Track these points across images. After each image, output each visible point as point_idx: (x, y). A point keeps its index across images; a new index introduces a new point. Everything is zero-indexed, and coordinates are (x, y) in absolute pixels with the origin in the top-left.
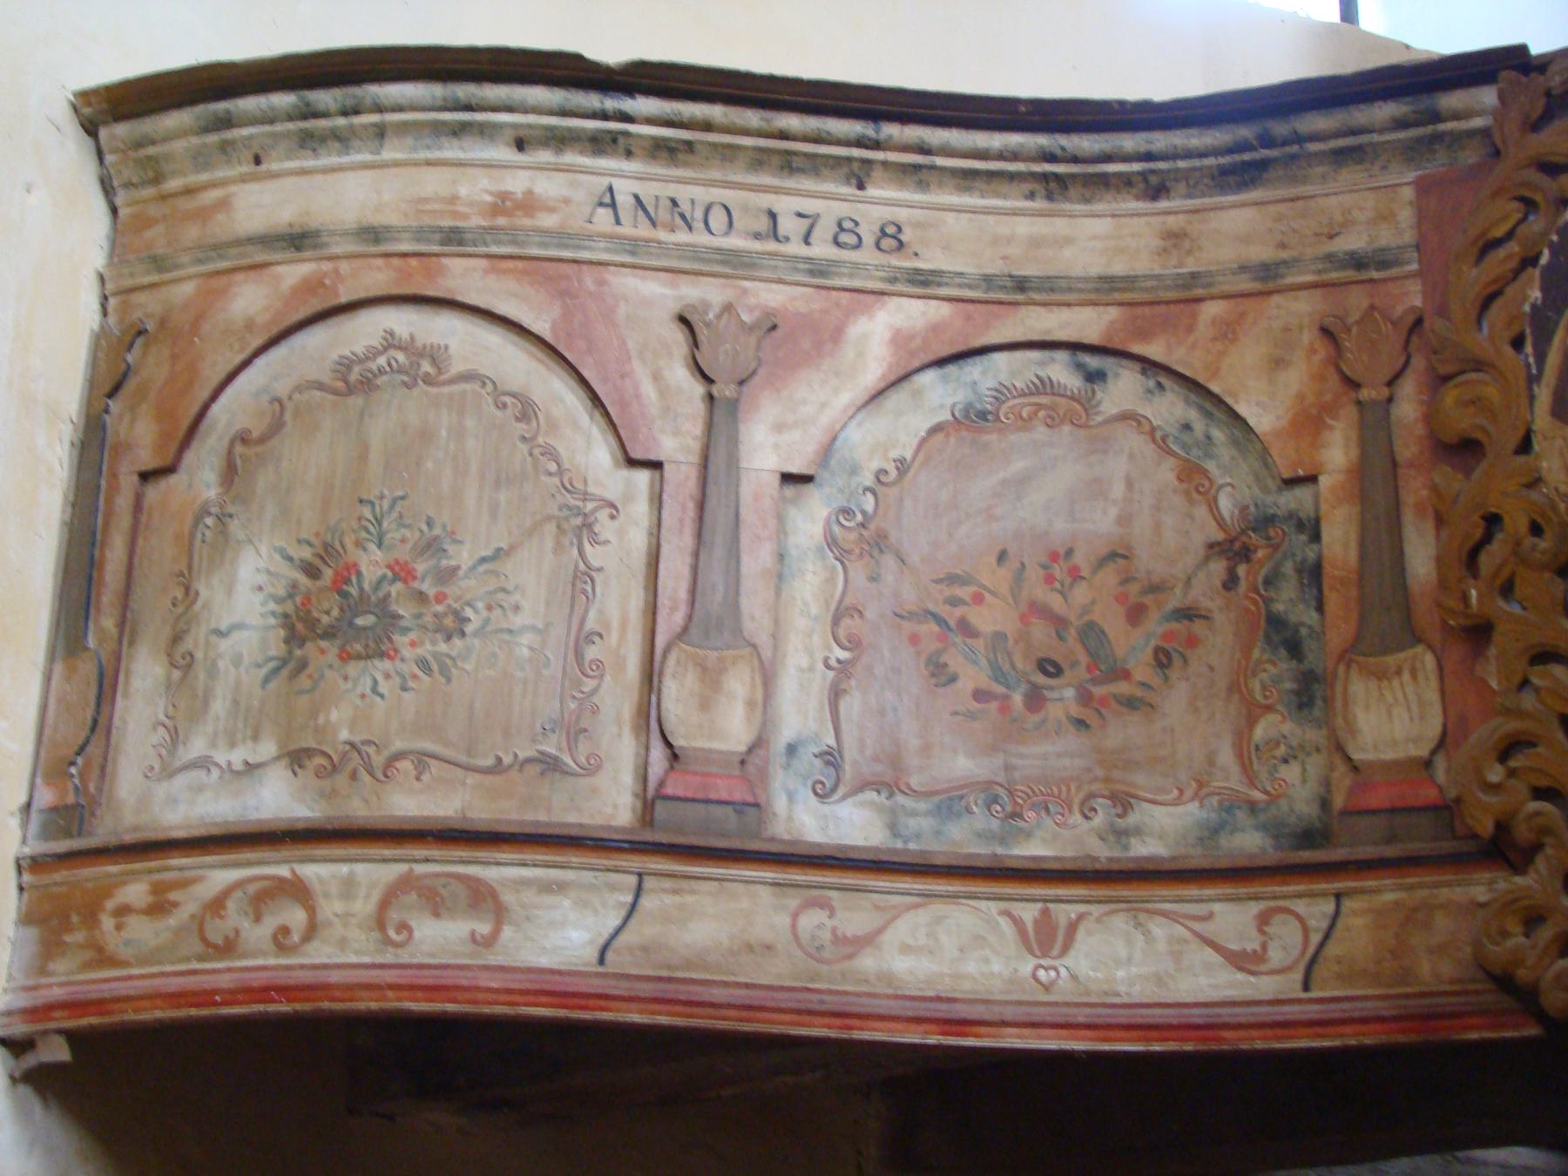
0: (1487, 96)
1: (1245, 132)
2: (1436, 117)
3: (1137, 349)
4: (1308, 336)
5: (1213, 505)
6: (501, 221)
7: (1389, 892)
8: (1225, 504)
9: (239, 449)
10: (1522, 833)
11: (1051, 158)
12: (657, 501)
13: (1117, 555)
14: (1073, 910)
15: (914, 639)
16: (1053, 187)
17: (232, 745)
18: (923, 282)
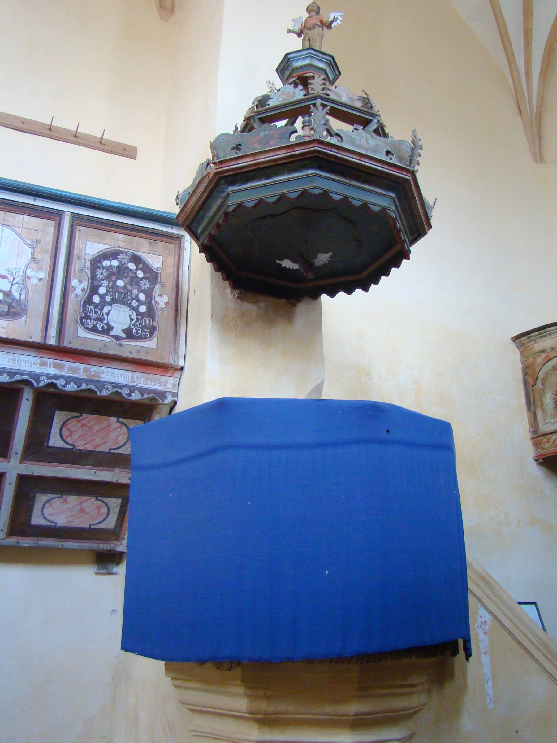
9: (543, 380)
17: (552, 419)
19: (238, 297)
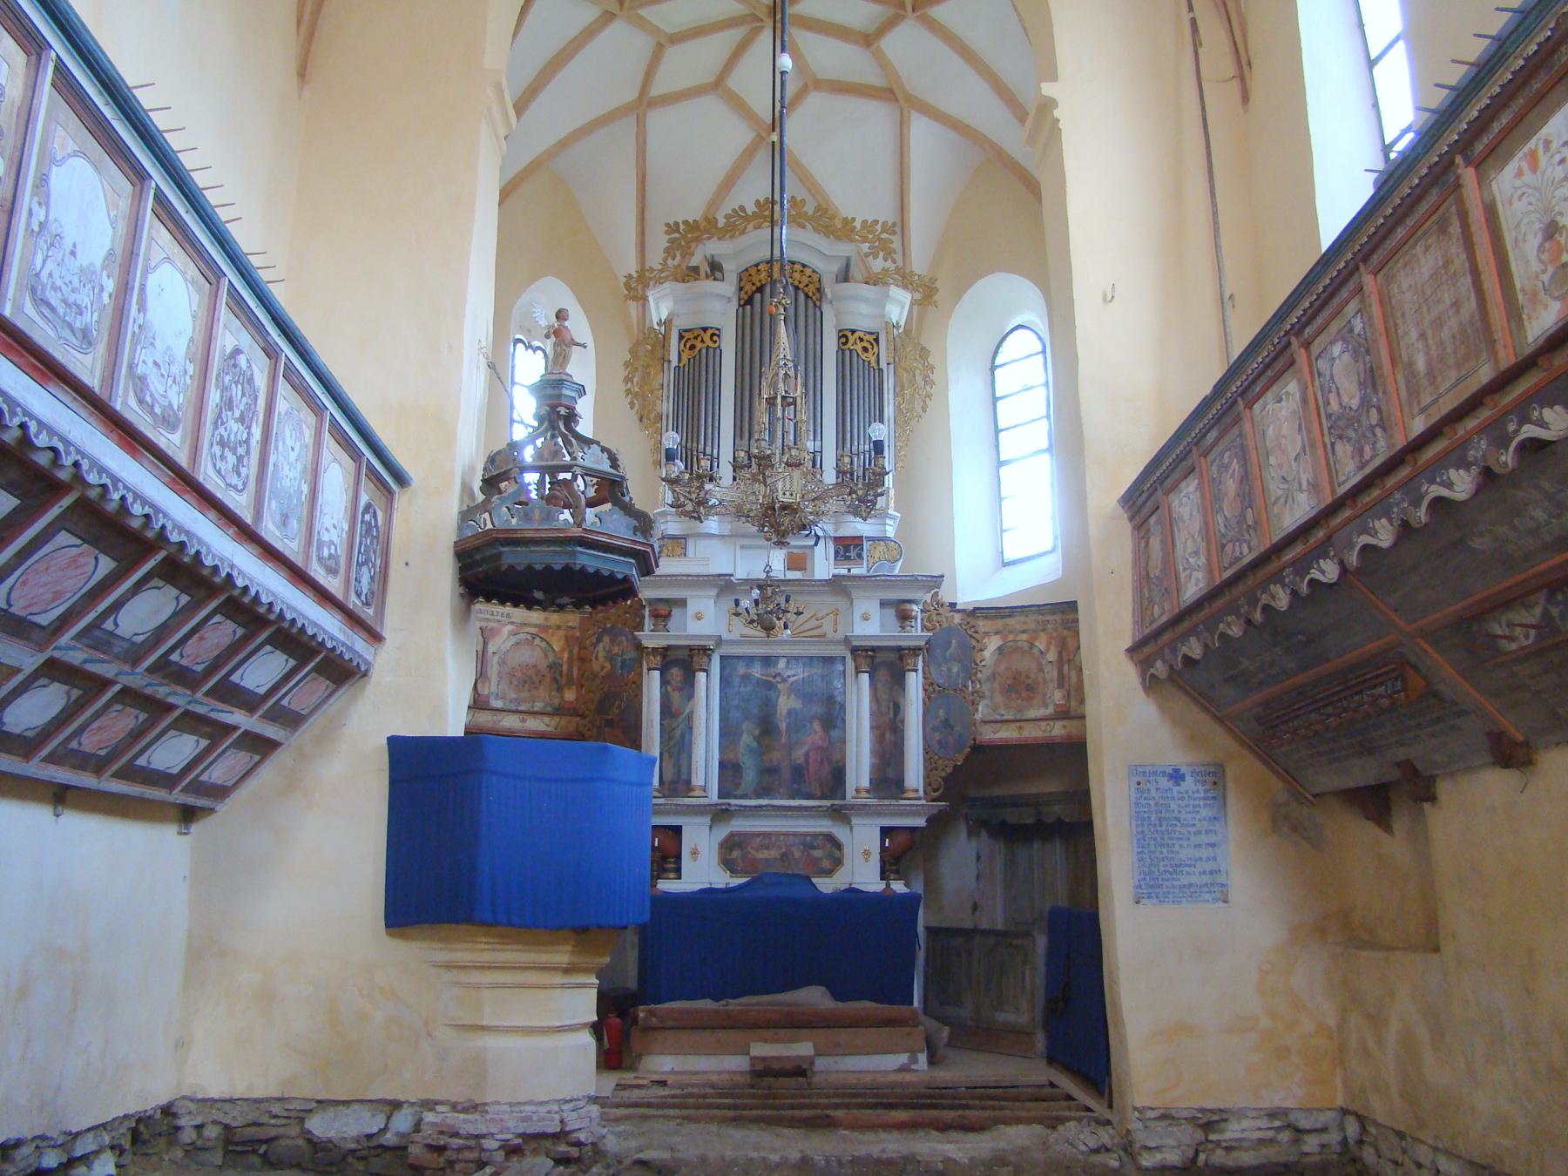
13: (535, 666)
18: (512, 623)
19: (462, 595)
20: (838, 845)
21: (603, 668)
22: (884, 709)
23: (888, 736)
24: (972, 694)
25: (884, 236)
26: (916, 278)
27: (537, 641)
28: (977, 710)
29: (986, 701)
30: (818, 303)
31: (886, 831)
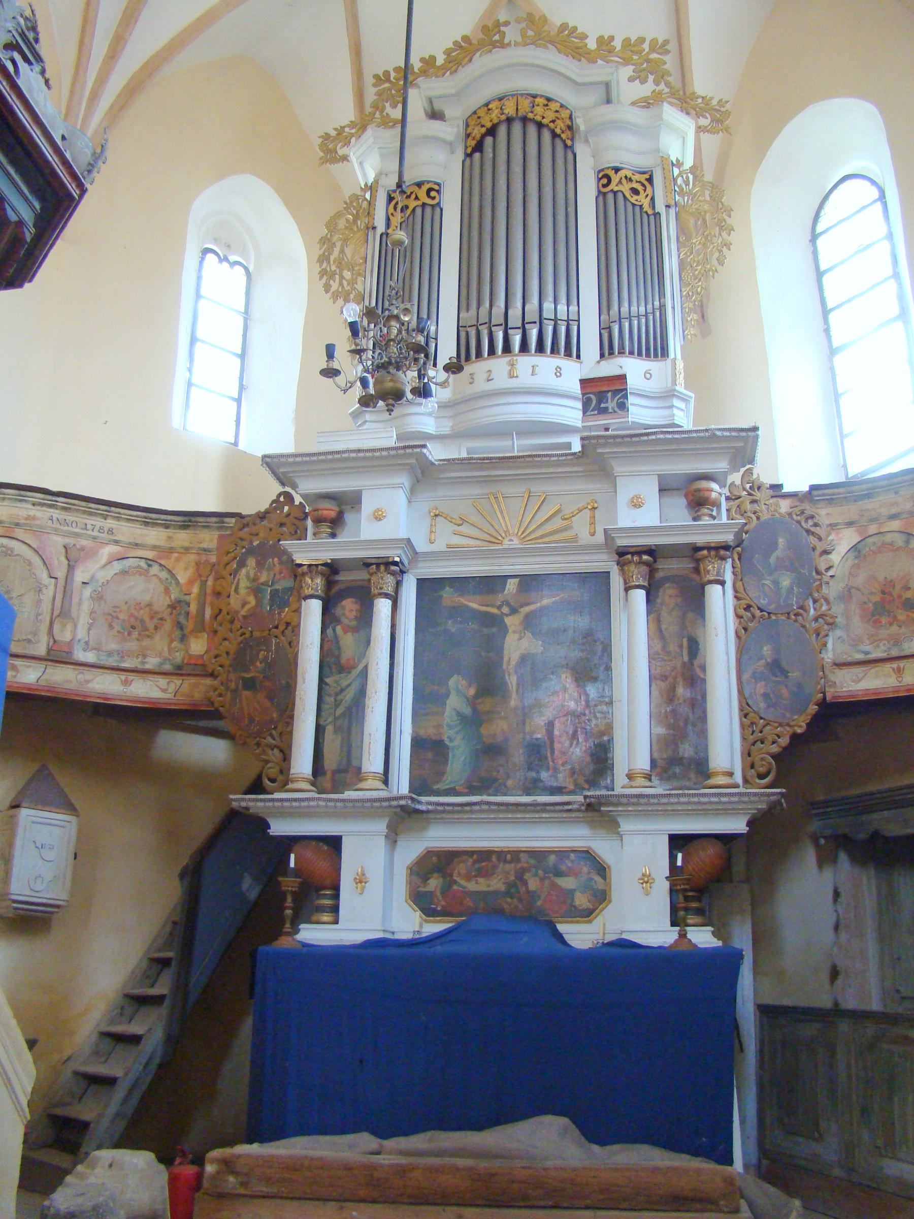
0: (233, 520)
1: (186, 519)
2: (223, 522)
3: (159, 561)
4: (193, 564)
5: (170, 597)
6: (28, 522)
7: (193, 680)
8: (173, 597)
10: (216, 673)
11: (146, 518)
12: (56, 585)
13: (149, 605)
14: (132, 678)
15: (106, 619)
16: (146, 524)
18: (116, 542)
20: (602, 870)
21: (244, 604)
22: (672, 647)
23: (680, 690)
24: (816, 619)
25: (654, 56)
26: (700, 100)
27: (155, 569)
28: (825, 645)
29: (838, 633)
30: (569, 143)
31: (677, 842)
